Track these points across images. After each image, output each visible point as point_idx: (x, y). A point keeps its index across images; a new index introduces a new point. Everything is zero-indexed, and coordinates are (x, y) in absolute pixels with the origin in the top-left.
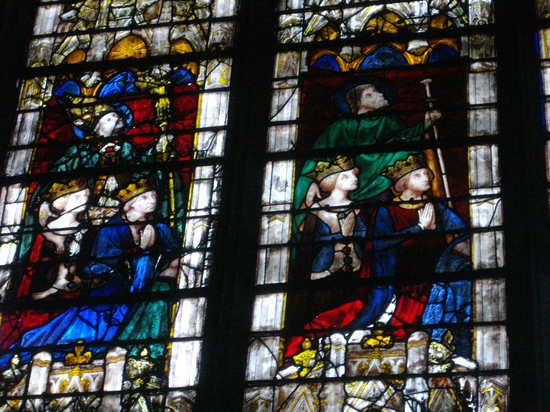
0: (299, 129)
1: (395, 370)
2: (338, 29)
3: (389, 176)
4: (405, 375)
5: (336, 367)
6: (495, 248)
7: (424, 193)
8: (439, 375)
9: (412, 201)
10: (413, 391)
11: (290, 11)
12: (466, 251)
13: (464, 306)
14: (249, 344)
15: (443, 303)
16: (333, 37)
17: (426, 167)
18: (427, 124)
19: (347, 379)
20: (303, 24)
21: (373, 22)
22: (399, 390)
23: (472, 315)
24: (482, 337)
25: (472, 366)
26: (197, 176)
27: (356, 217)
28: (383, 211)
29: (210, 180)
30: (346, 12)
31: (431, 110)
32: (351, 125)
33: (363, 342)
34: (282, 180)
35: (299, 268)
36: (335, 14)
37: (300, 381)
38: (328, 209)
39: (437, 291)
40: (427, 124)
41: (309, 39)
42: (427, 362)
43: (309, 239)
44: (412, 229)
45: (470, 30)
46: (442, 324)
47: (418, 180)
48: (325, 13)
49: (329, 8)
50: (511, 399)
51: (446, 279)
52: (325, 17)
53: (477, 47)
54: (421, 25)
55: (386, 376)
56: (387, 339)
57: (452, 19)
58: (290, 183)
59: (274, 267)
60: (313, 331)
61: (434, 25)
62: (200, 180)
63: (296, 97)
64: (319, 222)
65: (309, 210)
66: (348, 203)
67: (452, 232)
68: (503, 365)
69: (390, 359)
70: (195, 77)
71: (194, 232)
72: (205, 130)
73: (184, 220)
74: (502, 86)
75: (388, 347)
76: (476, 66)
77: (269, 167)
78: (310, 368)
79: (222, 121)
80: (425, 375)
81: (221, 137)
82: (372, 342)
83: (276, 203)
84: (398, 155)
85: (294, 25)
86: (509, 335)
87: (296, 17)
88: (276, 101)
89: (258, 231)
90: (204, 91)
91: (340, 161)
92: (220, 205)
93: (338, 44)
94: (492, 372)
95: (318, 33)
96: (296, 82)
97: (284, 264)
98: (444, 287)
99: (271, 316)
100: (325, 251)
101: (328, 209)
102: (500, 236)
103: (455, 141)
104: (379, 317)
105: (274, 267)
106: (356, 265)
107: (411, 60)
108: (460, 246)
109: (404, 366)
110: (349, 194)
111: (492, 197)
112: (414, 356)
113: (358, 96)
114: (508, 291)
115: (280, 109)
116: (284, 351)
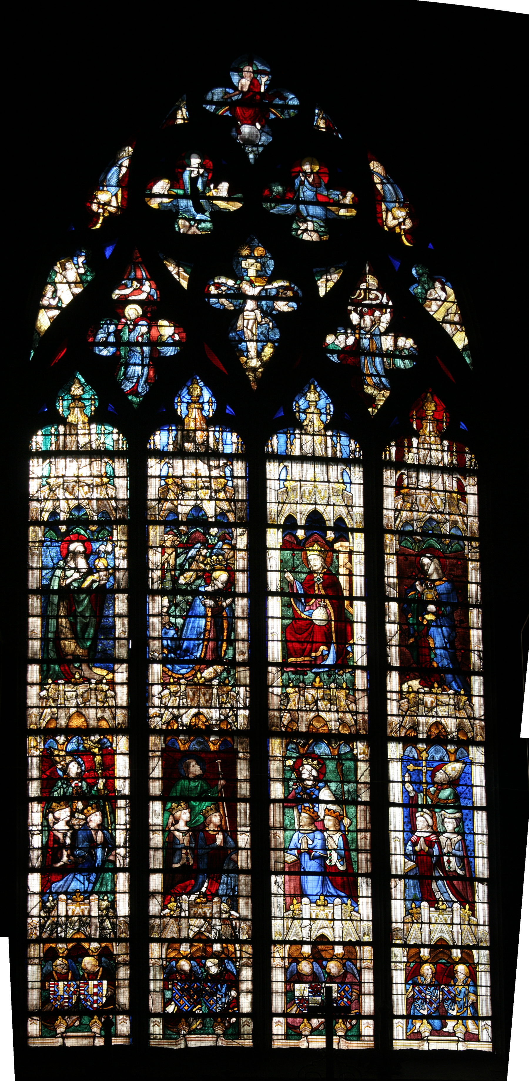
0: (163, 783)
1: (208, 915)
2: (177, 722)
3: (204, 815)
4: (212, 917)
5: (185, 911)
6: (247, 858)
7: (218, 826)
8: (225, 918)
9: (214, 831)
10: (215, 925)
11: (154, 707)
12: (236, 859)
13: (235, 886)
14: (149, 897)
15: (226, 884)
16: (175, 727)
17: (219, 812)
18: (220, 787)
19: (189, 917)
20: (161, 716)
21: (194, 720)
22: (210, 924)
23: (238, 892)
24: (242, 902)
25: (238, 915)
26: (119, 806)
27: (190, 836)
28: (202, 834)
29: (125, 808)
30: (182, 711)
31: (221, 779)
32: (185, 783)
33: (195, 900)
34: (157, 812)
35: (167, 860)
36: (175, 711)
37: (171, 917)
38: (178, 831)
39: (224, 878)
40: (220, 787)
41: (164, 727)
42: (220, 912)
43: (170, 846)
44: (212, 845)
45: (239, 733)
46: (226, 895)
47: (216, 819)
48: (171, 710)
49: (173, 708)
50: (253, 932)
51: (228, 872)
52: (171, 713)
53: (241, 744)
54: (216, 725)
55: (205, 917)
56: (205, 900)
57: (230, 723)
58: (161, 813)
59: (156, 860)
60: (175, 893)
61: (222, 726)
62: (120, 808)
63: (160, 762)
64: (174, 837)
65: (170, 830)
66: (187, 828)
67: (230, 849)
68: (250, 917)
69: (206, 910)
70: (112, 743)
71: (120, 837)
72: (119, 778)
73: (115, 829)
74: (252, 769)
75: (205, 903)
76: (241, 755)
77: (151, 803)
78: (175, 911)
79: (127, 774)
80: (220, 918)
81: (127, 781)
82: (198, 900)
83: (155, 825)
84: (207, 804)
85: (157, 716)
86: (252, 903)
87: (157, 710)
88: (152, 764)
89: (148, 840)
90: (117, 754)
91: (182, 804)
92: (132, 822)
93: (177, 733)
94: (246, 919)
95: (168, 723)
96: (159, 753)
97: (161, 858)
98: (227, 877)
99: (157, 884)
100: (178, 852)
101: (178, 831)
102: (249, 852)
103: (232, 800)
104: (201, 888)
105: (156, 860)
106: (191, 863)
107: (212, 747)
108: (234, 856)
109: (211, 913)
110: (187, 823)
111: (247, 832)
112: (215, 909)
113: (188, 767)
114: (252, 880)
115: (153, 770)
116: (163, 902)
